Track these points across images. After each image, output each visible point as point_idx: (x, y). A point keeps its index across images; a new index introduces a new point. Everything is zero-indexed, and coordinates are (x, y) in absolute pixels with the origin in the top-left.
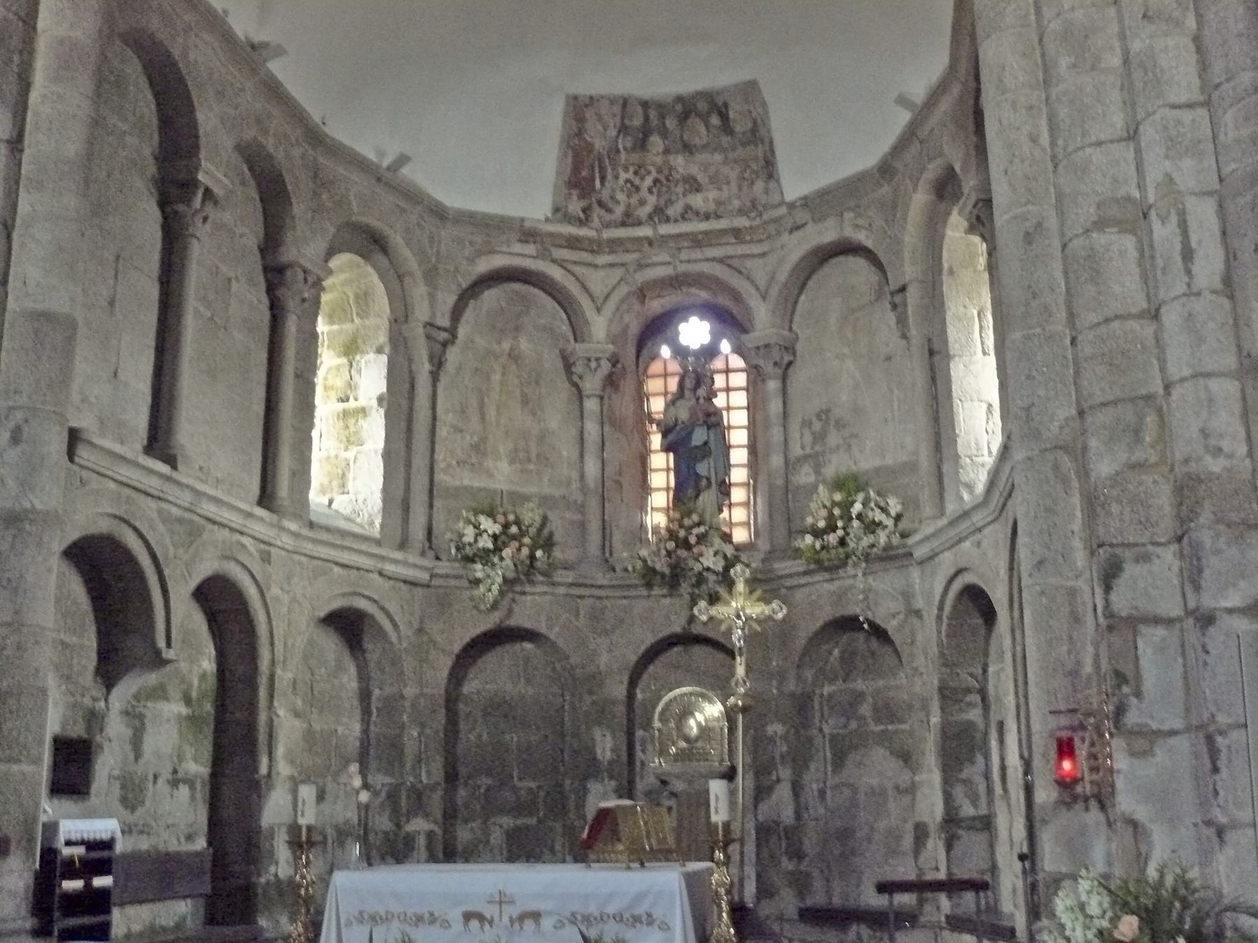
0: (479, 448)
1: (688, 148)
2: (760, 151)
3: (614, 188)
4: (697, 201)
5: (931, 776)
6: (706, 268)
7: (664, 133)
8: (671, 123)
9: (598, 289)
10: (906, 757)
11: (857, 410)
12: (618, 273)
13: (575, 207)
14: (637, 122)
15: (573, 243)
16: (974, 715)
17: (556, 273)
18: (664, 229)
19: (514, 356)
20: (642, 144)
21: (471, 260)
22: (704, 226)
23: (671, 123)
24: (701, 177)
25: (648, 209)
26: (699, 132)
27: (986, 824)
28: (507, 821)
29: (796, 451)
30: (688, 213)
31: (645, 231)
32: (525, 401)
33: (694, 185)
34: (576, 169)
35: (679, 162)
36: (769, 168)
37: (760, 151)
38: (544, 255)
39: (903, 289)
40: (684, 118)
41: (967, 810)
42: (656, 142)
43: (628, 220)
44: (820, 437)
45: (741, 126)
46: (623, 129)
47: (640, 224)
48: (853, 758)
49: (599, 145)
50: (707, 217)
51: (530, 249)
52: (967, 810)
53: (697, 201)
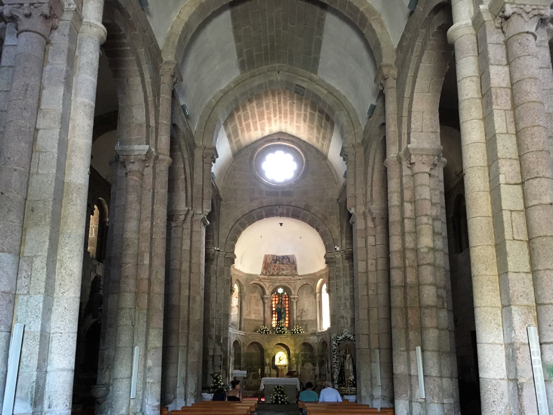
0: (250, 312)
1: (283, 263)
2: (294, 266)
3: (271, 269)
4: (284, 272)
5: (317, 368)
6: (285, 284)
7: (279, 261)
8: (280, 259)
9: (267, 286)
10: (314, 365)
11: (308, 310)
12: (271, 283)
13: (264, 272)
14: (275, 259)
15: (264, 279)
16: (324, 359)
17: (262, 284)
18: (279, 277)
19: (255, 297)
20: (276, 262)
21: (250, 282)
22: (285, 277)
23: (280, 259)
24: (285, 268)
25: (275, 273)
26: (285, 261)
27: (325, 375)
28: (253, 373)
29: (298, 315)
30: (281, 275)
31: (275, 277)
32: (256, 304)
33: (283, 270)
34: (265, 266)
35: (281, 265)
36: (296, 269)
37: (294, 266)
38: (260, 280)
39: (316, 294)
40: (282, 259)
41: (322, 373)
42: (278, 262)
43: (272, 275)
44: (302, 313)
45: (292, 261)
46: (273, 260)
47: (274, 275)
48: (305, 364)
49: (269, 262)
50: (285, 276)
51: (258, 280)
52: (322, 373)
53: (284, 272)
